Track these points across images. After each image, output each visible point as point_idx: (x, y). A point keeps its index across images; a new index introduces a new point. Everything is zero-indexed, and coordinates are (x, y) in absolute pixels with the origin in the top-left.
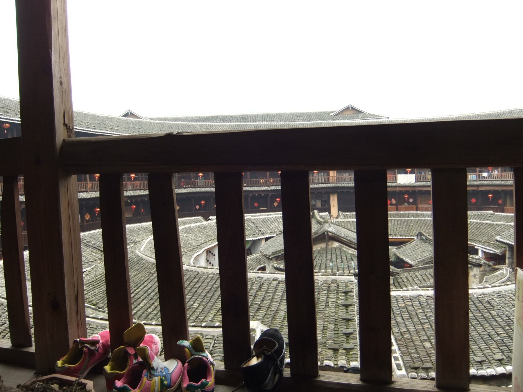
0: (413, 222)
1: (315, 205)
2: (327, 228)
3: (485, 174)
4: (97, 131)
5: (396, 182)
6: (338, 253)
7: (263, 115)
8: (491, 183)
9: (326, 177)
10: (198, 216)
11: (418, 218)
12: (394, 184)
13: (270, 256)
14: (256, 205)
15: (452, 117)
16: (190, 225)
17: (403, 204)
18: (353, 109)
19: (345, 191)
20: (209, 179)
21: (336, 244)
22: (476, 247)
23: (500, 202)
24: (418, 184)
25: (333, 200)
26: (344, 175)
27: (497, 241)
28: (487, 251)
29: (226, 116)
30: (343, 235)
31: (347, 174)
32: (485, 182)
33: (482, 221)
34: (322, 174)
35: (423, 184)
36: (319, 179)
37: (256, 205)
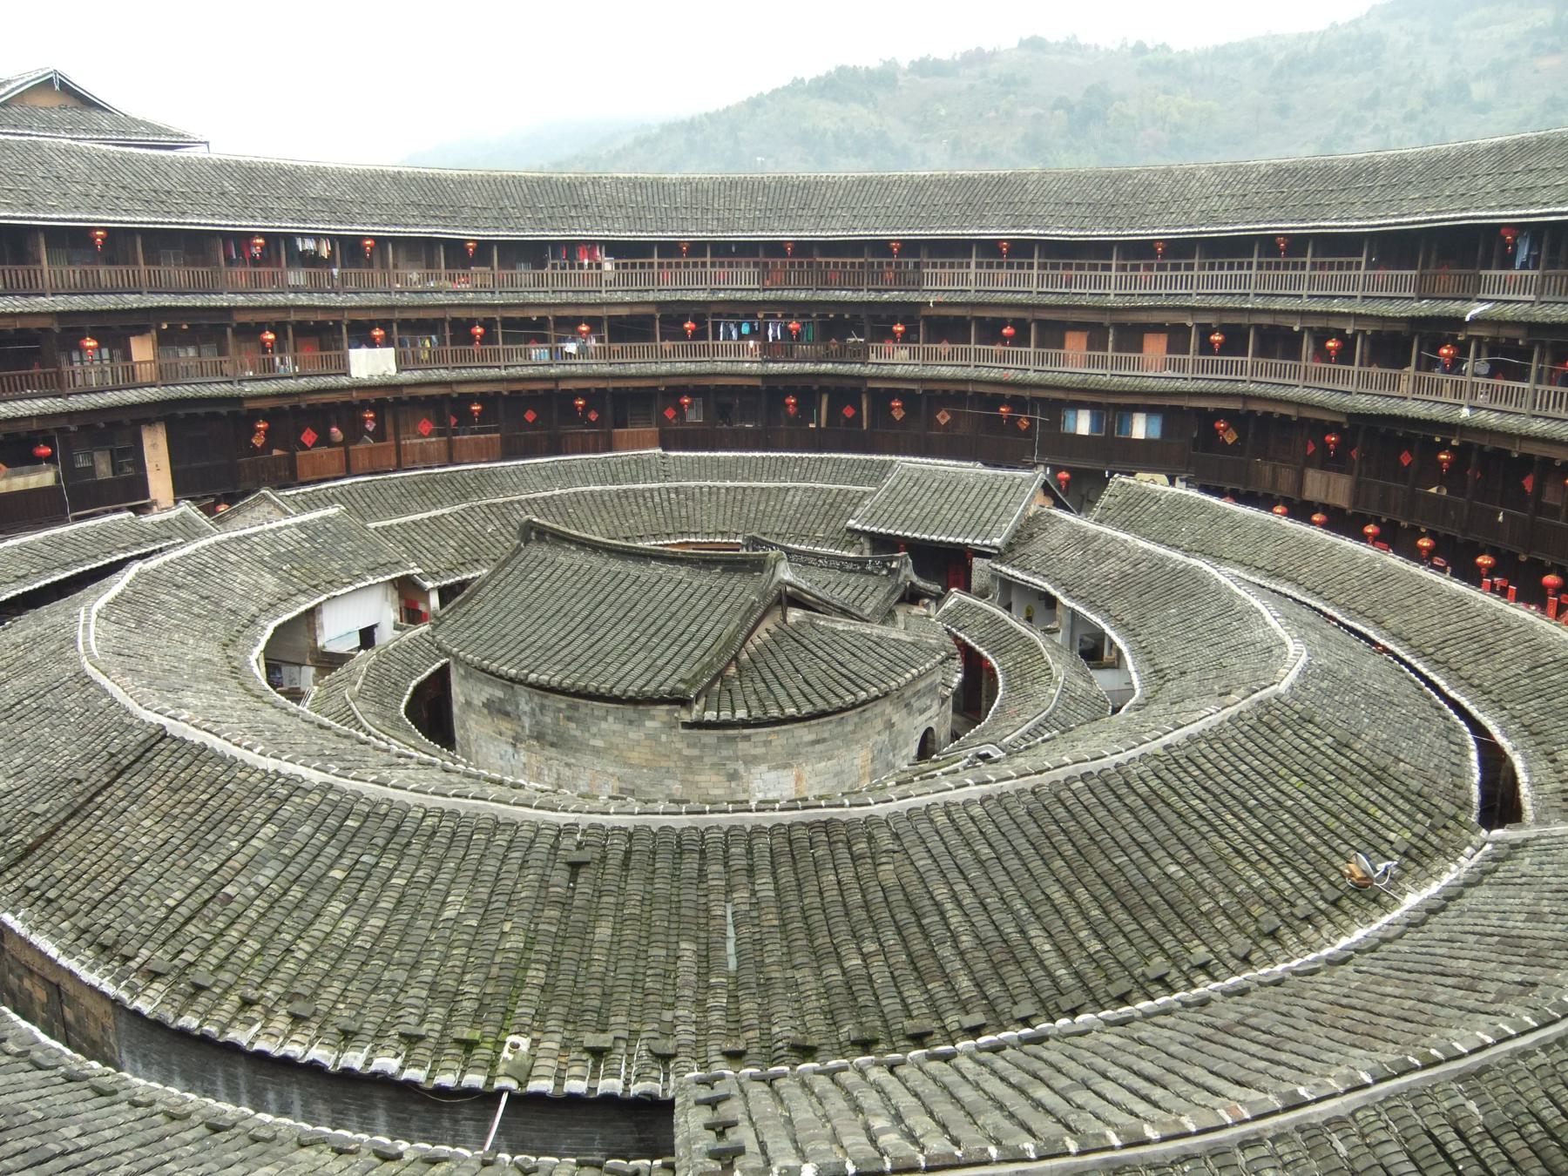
1: (91, 471)
3: (571, 348)
5: (347, 374)
9: (119, 364)
12: (344, 381)
19: (201, 411)
24: (406, 376)
25: (154, 445)
26: (182, 354)
27: (850, 530)
31: (191, 352)
32: (573, 368)
33: (736, 484)
34: (105, 352)
35: (417, 375)
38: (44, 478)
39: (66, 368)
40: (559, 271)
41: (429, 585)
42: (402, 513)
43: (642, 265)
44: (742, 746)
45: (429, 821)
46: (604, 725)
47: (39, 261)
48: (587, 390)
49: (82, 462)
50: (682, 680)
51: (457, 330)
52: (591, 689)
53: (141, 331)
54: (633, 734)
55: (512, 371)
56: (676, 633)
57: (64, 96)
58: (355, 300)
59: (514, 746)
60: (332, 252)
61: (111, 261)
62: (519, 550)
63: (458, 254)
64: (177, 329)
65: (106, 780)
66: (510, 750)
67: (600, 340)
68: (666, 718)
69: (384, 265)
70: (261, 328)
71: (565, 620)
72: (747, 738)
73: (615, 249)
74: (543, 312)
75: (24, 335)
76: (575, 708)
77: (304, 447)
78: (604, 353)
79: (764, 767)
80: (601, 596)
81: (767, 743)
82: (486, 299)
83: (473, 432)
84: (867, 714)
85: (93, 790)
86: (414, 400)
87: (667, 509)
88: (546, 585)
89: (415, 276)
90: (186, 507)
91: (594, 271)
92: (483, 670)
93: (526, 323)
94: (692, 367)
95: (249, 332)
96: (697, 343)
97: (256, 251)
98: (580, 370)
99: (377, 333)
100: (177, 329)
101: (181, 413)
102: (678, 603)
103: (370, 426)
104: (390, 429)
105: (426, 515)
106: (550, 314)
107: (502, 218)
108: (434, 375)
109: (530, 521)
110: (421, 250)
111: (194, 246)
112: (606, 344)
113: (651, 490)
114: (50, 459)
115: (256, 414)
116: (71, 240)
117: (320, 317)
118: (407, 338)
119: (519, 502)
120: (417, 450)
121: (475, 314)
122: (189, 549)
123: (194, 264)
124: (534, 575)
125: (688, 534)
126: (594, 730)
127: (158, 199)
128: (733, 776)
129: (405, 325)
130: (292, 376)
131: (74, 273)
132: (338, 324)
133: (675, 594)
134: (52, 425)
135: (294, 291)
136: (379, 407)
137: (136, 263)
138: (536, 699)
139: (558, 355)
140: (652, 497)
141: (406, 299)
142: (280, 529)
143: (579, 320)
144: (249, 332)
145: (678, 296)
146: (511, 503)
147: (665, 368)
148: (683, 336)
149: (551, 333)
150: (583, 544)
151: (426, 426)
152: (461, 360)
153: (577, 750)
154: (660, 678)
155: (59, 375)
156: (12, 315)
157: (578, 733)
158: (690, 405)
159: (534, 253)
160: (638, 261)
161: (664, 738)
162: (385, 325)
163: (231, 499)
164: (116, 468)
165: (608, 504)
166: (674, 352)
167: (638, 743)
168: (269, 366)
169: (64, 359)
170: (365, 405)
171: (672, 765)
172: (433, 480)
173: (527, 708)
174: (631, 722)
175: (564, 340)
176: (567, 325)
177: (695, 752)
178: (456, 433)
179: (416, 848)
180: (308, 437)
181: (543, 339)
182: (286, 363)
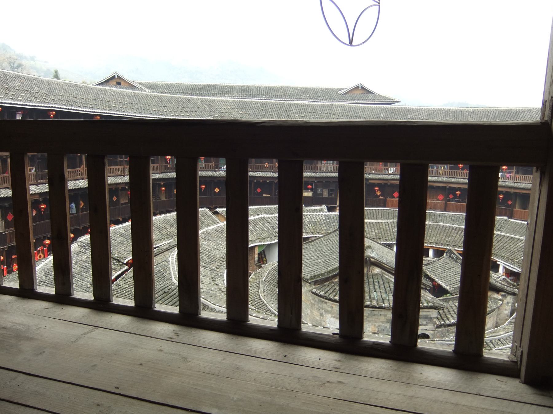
0: (431, 228)
1: (322, 194)
2: (369, 254)
4: (96, 111)
6: (381, 281)
7: (266, 87)
10: (203, 207)
11: (437, 223)
13: (308, 280)
14: (259, 190)
15: (469, 109)
16: (207, 229)
18: (363, 88)
20: (211, 162)
21: (377, 270)
22: (498, 263)
23: (510, 203)
28: (510, 268)
29: (225, 86)
30: (385, 262)
36: (327, 167)
37: (259, 190)
44: (325, 305)
49: (320, 191)
57: (362, 91)
72: (326, 303)
79: (330, 315)
81: (332, 307)
83: (456, 201)
84: (375, 313)
86: (438, 187)
105: (376, 221)
114: (311, 189)
120: (433, 205)
128: (321, 315)
134: (311, 180)
152: (451, 175)
155: (315, 167)
164: (330, 194)
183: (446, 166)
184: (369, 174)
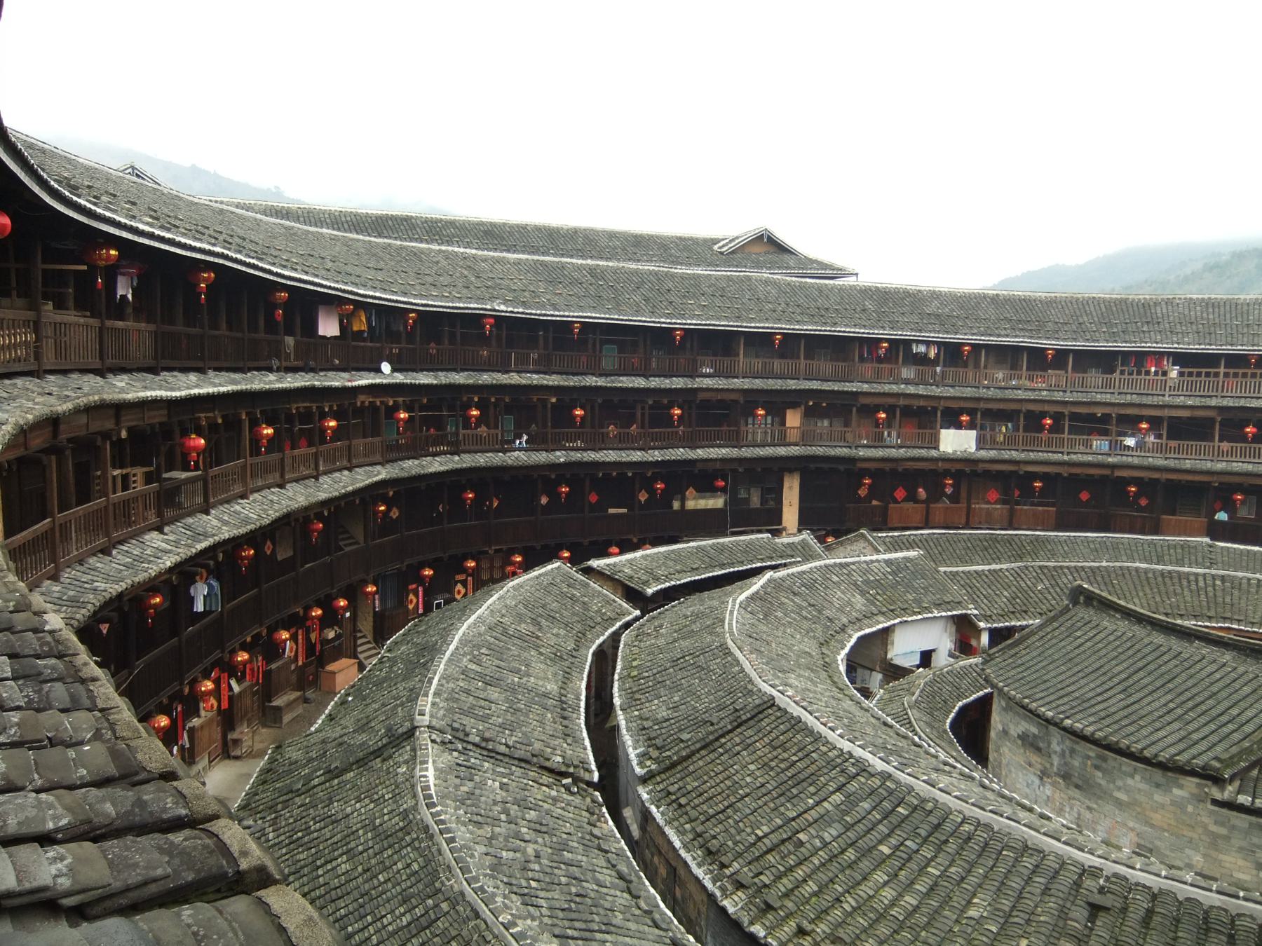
1: (747, 501)
3: (1130, 442)
5: (937, 448)
8: (1146, 462)
9: (777, 428)
12: (934, 453)
15: (1038, 295)
17: (937, 500)
19: (825, 466)
25: (791, 488)
31: (826, 423)
32: (1130, 459)
34: (769, 418)
38: (717, 502)
39: (743, 428)
40: (1126, 376)
41: (982, 625)
42: (966, 563)
43: (1208, 374)
45: (966, 827)
46: (1130, 781)
47: (738, 355)
48: (1141, 479)
49: (742, 494)
50: (1216, 758)
51: (1030, 420)
52: (1122, 745)
53: (794, 405)
54: (1158, 797)
55: (1073, 457)
56: (1214, 712)
57: (769, 246)
58: (951, 392)
59: (1041, 779)
60: (938, 355)
61: (782, 356)
62: (1066, 610)
63: (1038, 360)
64: (822, 406)
65: (729, 727)
66: (1037, 781)
67: (1159, 436)
68: (1195, 791)
69: (977, 366)
70: (877, 408)
71: (1104, 678)
73: (1181, 359)
74: (1107, 410)
75: (723, 404)
76: (1104, 759)
77: (896, 501)
78: (1160, 449)
80: (1141, 664)
82: (1058, 396)
83: (1033, 504)
85: (720, 732)
86: (987, 473)
87: (1211, 594)
88: (1089, 644)
89: (1000, 375)
90: (806, 536)
91: (1160, 377)
92: (1023, 707)
93: (1091, 418)
94: (1250, 467)
95: (869, 412)
96: (1257, 446)
97: (882, 352)
98: (1136, 461)
99: (964, 418)
100: (822, 406)
101: (812, 466)
102: (1220, 685)
103: (949, 491)
104: (964, 494)
105: (987, 567)
106: (1114, 412)
107: (1080, 332)
108: (1006, 455)
109: (1081, 586)
110: (1008, 356)
111: (838, 347)
112: (1164, 441)
113: (1196, 575)
114: (723, 490)
115: (864, 473)
116: (759, 341)
117: (922, 403)
118: (988, 423)
119: (1068, 568)
121: (1046, 408)
122: (805, 567)
123: (837, 360)
124: (1079, 633)
125: (1231, 620)
126: (1120, 783)
127: (819, 314)
129: (988, 414)
130: (896, 447)
131: (758, 364)
132: (935, 409)
133: (1217, 676)
135: (905, 383)
136: (958, 476)
137: (798, 358)
138: (1068, 742)
139: (1117, 447)
140: (1197, 581)
141: (991, 393)
142: (872, 562)
143: (1140, 419)
144: (869, 412)
145: (1242, 403)
146: (1061, 567)
147: (1220, 466)
148: (1244, 438)
149: (1113, 428)
150: (1128, 614)
151: (993, 495)
153: (1100, 798)
154: (1194, 751)
155: (738, 432)
156: (717, 390)
157: (1103, 782)
158: (1243, 502)
159: (1105, 361)
160: (1204, 370)
161: (1190, 809)
162: (972, 412)
163: (838, 534)
164: (764, 501)
165: (1152, 581)
166: (1231, 453)
167: (1163, 806)
168: (879, 437)
169: (743, 422)
170: (947, 473)
171: (1195, 836)
172: (995, 539)
173: (1058, 749)
174: (1158, 786)
175: (1125, 435)
176: (1129, 422)
177: (1223, 831)
178: (1018, 504)
179: (952, 847)
180: (900, 494)
181: (1105, 433)
182: (892, 437)
183: (1010, 425)
184: (857, 447)
